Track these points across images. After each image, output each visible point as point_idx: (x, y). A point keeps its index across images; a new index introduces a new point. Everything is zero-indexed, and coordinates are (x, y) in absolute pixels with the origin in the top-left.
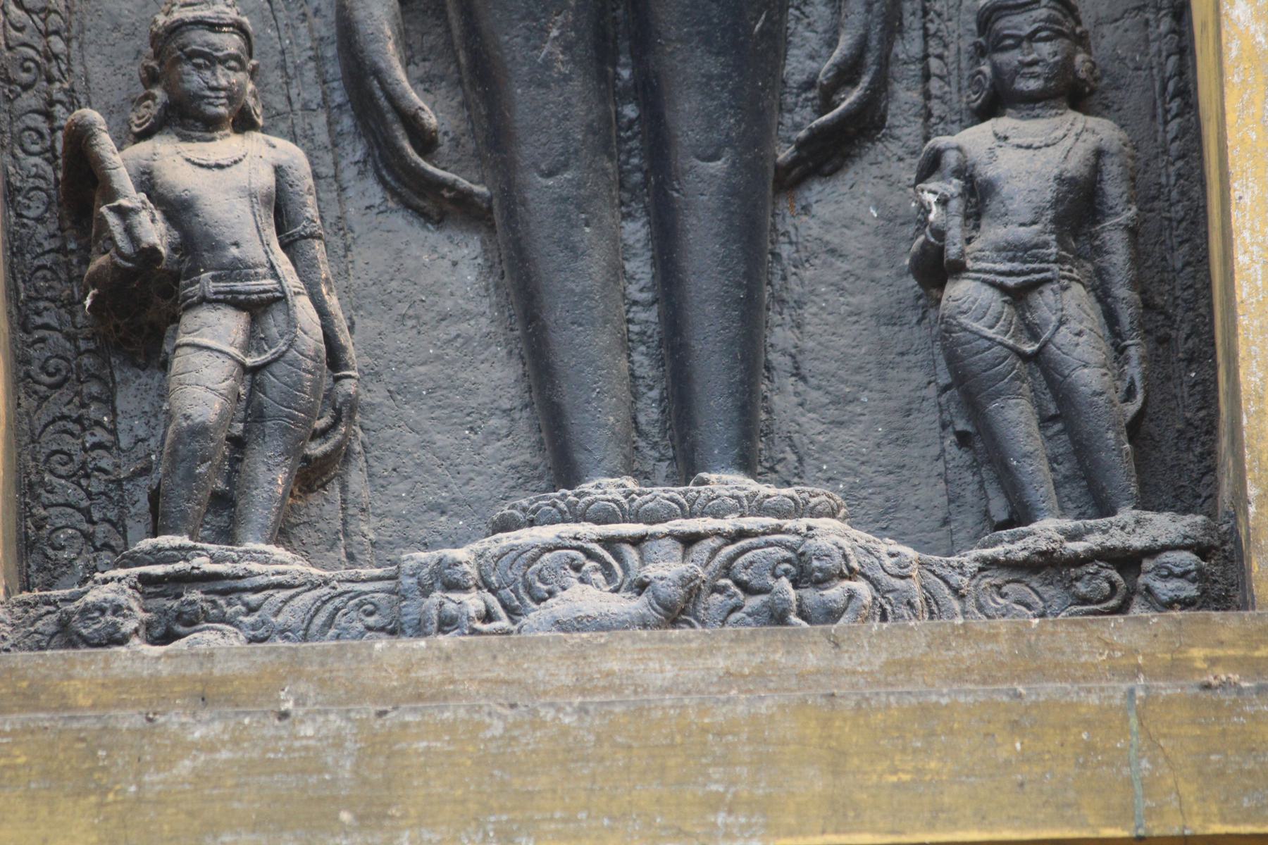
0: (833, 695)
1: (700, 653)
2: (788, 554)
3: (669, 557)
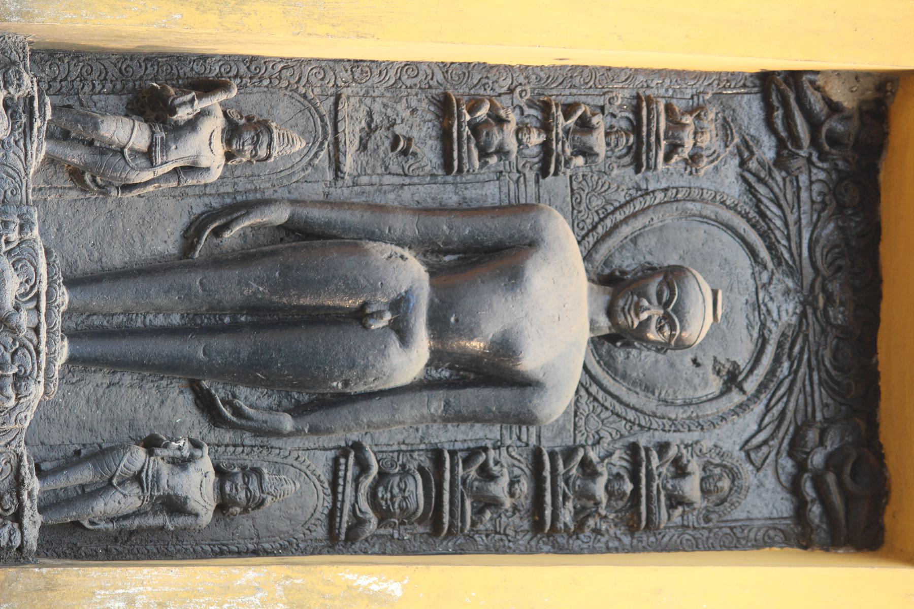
2: (28, 372)
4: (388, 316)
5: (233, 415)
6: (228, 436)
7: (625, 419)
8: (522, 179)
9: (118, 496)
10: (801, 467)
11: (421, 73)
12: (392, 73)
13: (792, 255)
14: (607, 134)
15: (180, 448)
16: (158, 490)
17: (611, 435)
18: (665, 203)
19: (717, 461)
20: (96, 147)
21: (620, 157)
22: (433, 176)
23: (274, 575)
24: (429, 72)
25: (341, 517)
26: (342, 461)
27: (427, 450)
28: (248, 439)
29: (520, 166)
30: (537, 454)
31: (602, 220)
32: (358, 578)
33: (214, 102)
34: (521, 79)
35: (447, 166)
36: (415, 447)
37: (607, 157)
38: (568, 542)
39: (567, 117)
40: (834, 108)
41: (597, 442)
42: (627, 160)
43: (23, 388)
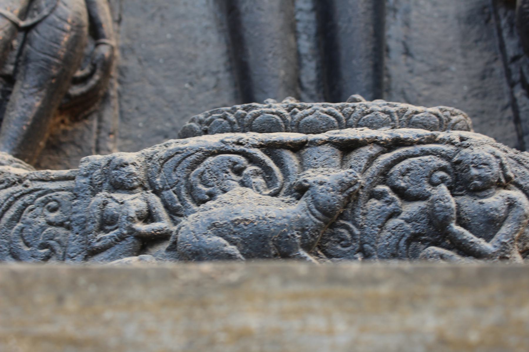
2: (444, 163)
3: (326, 163)
20: (16, 71)
43: (484, 172)
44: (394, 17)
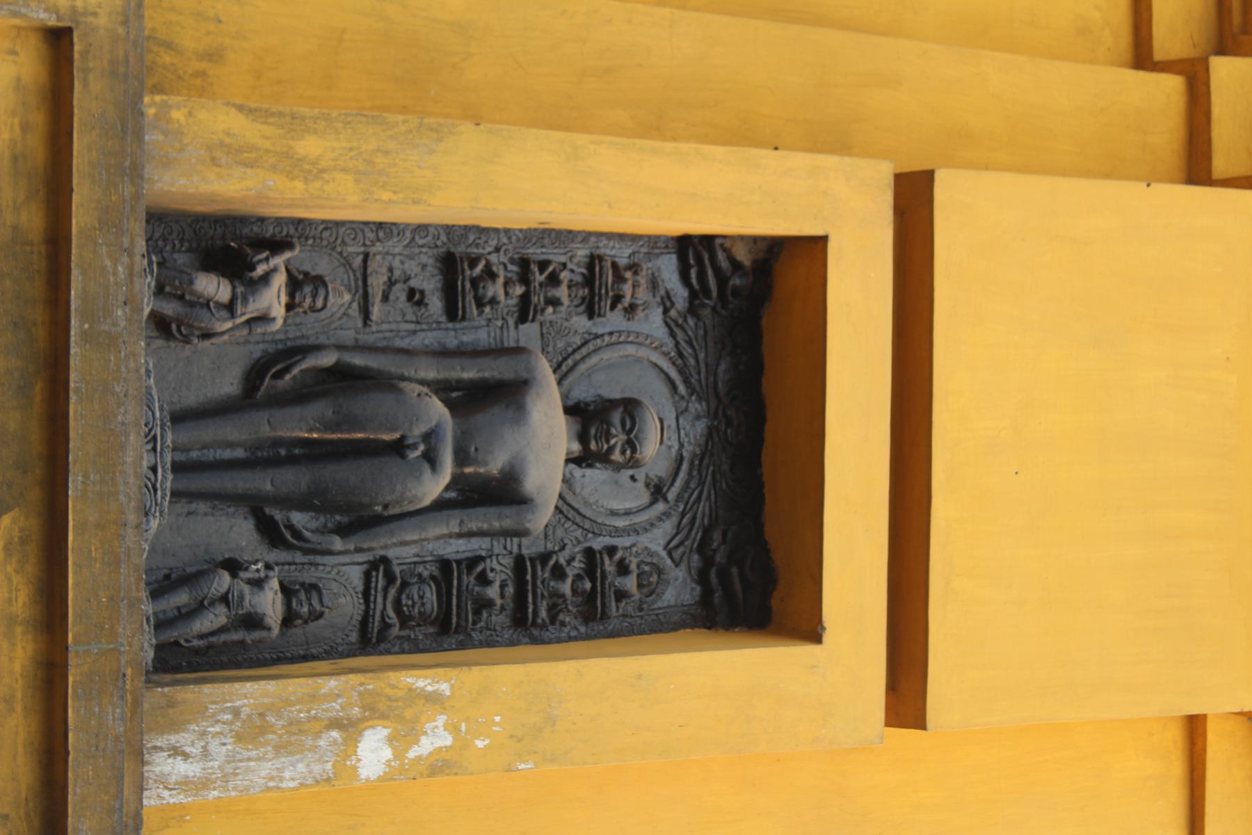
0: (126, 525)
1: (136, 472)
3: (149, 461)
4: (422, 447)
5: (292, 537)
6: (284, 556)
7: (583, 528)
8: (505, 326)
9: (211, 616)
10: (708, 563)
11: (430, 234)
12: (408, 234)
13: (701, 387)
14: (569, 287)
15: (258, 571)
16: (242, 609)
17: (571, 541)
18: (612, 344)
19: (648, 560)
20: (186, 301)
21: (577, 306)
22: (439, 323)
23: (351, 683)
24: (436, 233)
25: (373, 623)
26: (374, 574)
27: (436, 561)
28: (299, 557)
29: (505, 312)
30: (519, 562)
31: (565, 359)
32: (416, 681)
33: (279, 261)
34: (505, 240)
35: (452, 312)
36: (426, 559)
37: (569, 306)
38: (540, 634)
39: (541, 272)
40: (736, 265)
41: (563, 548)
42: (582, 308)
44: (210, 508)
